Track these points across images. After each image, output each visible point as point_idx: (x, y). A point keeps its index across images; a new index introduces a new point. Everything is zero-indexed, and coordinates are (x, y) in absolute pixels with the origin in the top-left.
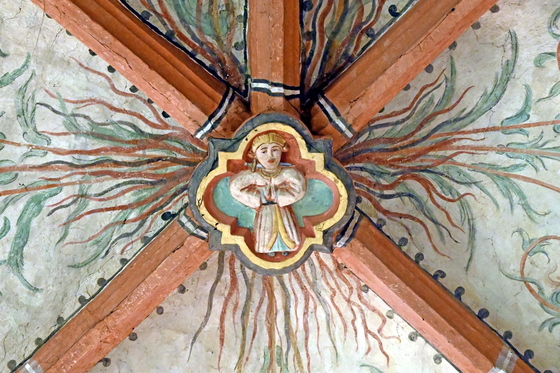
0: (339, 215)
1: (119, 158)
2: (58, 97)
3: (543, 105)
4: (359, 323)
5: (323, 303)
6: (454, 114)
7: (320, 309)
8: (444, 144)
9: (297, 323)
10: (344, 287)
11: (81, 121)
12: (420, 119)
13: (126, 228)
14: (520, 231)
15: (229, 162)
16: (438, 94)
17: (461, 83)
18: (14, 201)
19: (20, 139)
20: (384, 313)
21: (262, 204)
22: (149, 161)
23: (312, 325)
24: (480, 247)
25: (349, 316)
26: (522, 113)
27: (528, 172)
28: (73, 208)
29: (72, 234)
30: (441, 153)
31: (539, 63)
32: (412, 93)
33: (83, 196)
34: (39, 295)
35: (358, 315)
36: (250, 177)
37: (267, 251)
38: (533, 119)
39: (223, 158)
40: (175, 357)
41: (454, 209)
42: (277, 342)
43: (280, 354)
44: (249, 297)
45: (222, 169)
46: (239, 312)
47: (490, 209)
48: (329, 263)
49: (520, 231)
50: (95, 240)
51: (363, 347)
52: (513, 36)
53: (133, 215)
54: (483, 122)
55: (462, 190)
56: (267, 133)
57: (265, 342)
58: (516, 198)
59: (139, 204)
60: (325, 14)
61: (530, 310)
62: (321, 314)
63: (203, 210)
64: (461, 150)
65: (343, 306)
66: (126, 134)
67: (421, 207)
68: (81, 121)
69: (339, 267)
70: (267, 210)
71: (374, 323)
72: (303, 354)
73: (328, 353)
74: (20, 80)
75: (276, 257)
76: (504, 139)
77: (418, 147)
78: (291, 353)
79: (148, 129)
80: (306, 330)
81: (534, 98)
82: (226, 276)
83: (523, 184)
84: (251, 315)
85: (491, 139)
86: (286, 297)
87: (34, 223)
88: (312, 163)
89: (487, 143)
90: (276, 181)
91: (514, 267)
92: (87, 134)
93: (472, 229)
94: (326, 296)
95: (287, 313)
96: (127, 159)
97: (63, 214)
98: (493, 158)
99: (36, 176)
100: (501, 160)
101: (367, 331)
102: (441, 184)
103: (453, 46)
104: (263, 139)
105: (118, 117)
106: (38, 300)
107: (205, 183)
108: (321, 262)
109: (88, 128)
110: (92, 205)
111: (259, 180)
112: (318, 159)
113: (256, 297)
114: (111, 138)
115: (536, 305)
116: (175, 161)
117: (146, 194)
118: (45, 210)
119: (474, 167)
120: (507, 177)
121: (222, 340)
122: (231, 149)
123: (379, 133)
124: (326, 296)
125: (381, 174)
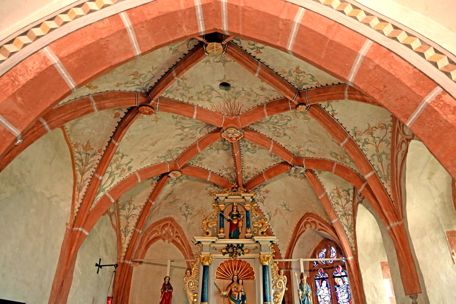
10: (219, 110)
23: (224, 105)
25: (218, 107)
44: (234, 107)
54: (202, 127)
62: (222, 106)
65: (219, 108)
70: (233, 133)
71: (214, 108)
76: (199, 126)
80: (224, 104)
85: (201, 126)
86: (228, 107)
88: (227, 139)
94: (222, 109)
113: (233, 107)
124: (222, 109)
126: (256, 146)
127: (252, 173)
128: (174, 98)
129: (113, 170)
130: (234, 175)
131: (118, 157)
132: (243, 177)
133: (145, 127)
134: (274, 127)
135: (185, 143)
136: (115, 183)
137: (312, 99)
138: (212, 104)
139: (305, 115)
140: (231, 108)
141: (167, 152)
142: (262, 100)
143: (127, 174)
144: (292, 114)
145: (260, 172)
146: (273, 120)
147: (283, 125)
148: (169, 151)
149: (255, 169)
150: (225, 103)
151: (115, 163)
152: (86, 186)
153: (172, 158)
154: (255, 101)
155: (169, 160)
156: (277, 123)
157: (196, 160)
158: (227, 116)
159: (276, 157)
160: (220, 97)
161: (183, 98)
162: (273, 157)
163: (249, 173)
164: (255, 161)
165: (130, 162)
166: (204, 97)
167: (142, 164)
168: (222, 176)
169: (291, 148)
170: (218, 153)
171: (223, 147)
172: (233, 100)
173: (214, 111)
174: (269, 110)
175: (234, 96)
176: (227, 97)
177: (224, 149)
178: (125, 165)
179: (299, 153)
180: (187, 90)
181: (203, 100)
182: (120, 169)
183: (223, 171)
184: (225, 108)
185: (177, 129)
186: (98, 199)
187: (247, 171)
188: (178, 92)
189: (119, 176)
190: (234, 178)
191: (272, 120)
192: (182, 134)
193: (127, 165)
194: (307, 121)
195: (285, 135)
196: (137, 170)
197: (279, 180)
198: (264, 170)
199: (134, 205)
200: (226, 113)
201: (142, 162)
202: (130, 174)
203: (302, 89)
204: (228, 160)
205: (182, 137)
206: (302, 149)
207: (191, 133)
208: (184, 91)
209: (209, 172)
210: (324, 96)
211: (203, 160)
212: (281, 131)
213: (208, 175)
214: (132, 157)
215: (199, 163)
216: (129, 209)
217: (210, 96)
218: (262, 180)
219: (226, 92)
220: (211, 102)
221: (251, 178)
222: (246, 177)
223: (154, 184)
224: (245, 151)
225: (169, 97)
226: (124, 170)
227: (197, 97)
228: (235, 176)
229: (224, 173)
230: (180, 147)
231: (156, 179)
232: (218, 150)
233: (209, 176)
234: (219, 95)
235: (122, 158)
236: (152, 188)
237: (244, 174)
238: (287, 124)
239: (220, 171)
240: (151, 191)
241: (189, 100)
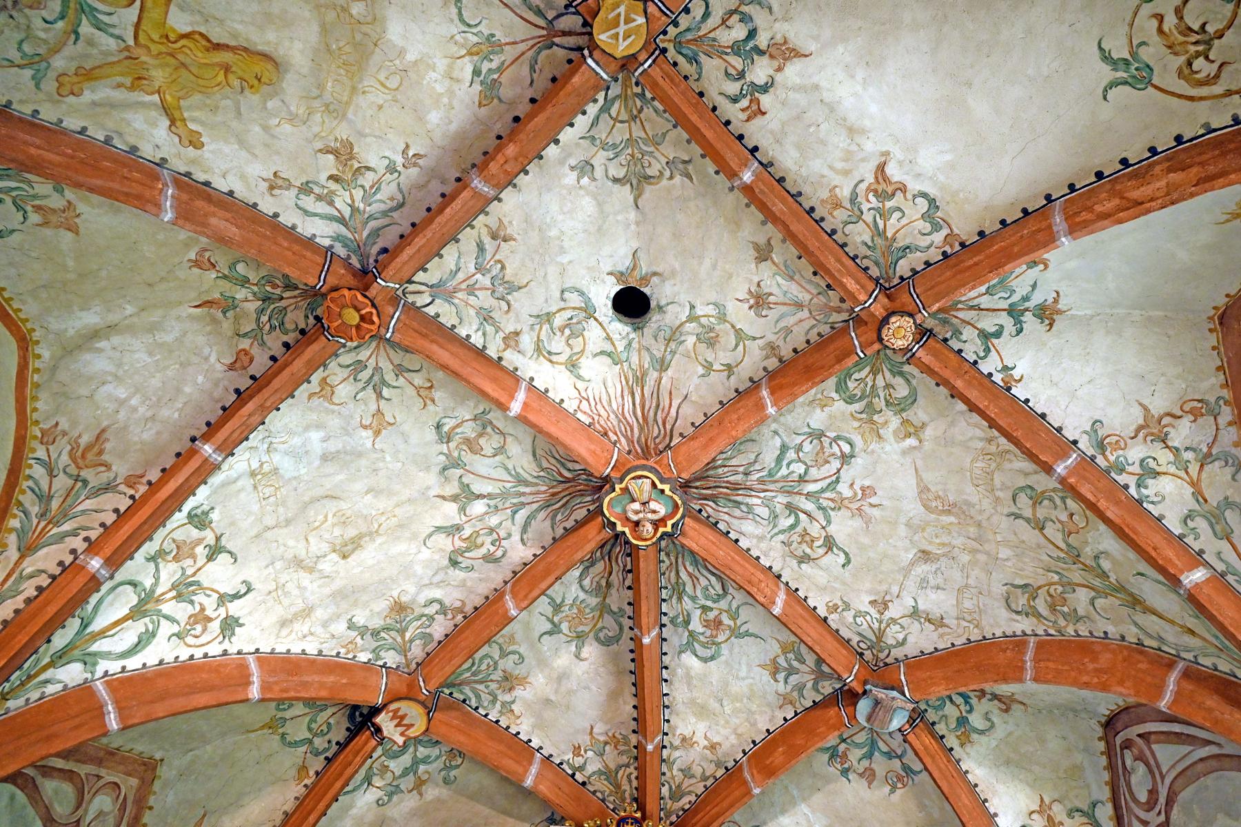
0: (607, 500)
1: (725, 490)
2: (756, 522)
3: (505, 518)
4: (593, 404)
5: (614, 412)
6: (550, 509)
7: (615, 409)
8: (553, 495)
9: (628, 399)
10: (602, 423)
11: (745, 510)
12: (568, 506)
13: (724, 456)
14: (508, 458)
15: (666, 526)
16: (559, 517)
17: (548, 523)
18: (783, 477)
19: (778, 505)
20: (579, 413)
21: (648, 502)
22: (710, 488)
23: (620, 400)
24: (529, 448)
25: (599, 407)
26: (515, 513)
27: (510, 485)
28: (752, 469)
29: (753, 457)
30: (555, 490)
31: (509, 535)
32: (573, 518)
33: (746, 474)
34: (773, 429)
35: (593, 408)
36: (655, 517)
37: (645, 480)
38: (509, 511)
39: (669, 529)
40: (697, 387)
41: (545, 464)
42: (639, 389)
43: (637, 382)
44: (656, 414)
45: (670, 523)
46: (661, 407)
47: (526, 466)
48: (611, 434)
49: (508, 458)
50: (740, 452)
51: (589, 391)
52: (524, 544)
53: (720, 462)
54: (535, 506)
55: (542, 474)
56: (646, 540)
57: (646, 388)
58: (513, 472)
59: (716, 468)
60: (620, 552)
61: (498, 419)
62: (615, 406)
63: (679, 502)
64: (544, 492)
66: (722, 502)
67: (563, 465)
68: (745, 510)
69: (606, 434)
72: (624, 383)
73: (609, 384)
74: (776, 530)
75: (640, 477)
76: (522, 499)
77: (567, 493)
78: (630, 383)
79: (711, 503)
80: (622, 396)
81: (510, 520)
82: (668, 427)
83: (510, 479)
84: (654, 405)
85: (530, 499)
87: (773, 465)
88: (623, 526)
89: (532, 497)
90: (641, 515)
91: (509, 439)
92: (742, 503)
93: (534, 455)
95: (634, 404)
96: (721, 490)
97: (757, 467)
98: (527, 490)
99: (771, 487)
100: (522, 489)
101: (588, 400)
102: (553, 476)
103: (554, 539)
104: (648, 537)
105: (725, 510)
106: (774, 426)
107: (678, 516)
108: (616, 434)
109: (742, 506)
110: (741, 469)
111: (650, 516)
112: (619, 528)
113: (652, 414)
114: (730, 500)
115: (495, 422)
116: (697, 488)
117: (711, 473)
118: (767, 470)
119: (537, 484)
120: (519, 481)
121: (671, 393)
122: (664, 534)
123: (589, 498)
124: (612, 416)
125: (586, 480)
126: (720, 623)
127: (697, 771)
128: (454, 326)
129: (159, 591)
130: (630, 781)
131: (200, 541)
132: (665, 791)
133: (333, 446)
134: (791, 508)
135: (463, 584)
136: (150, 657)
137: (936, 289)
138: (581, 385)
139: (904, 415)
140: (645, 418)
141: (392, 609)
142: (753, 361)
143: (209, 645)
144: (856, 424)
145: (730, 764)
146: (788, 465)
147: (823, 491)
148: (400, 608)
149: (713, 747)
150: (626, 393)
151: (176, 559)
152: (21, 598)
153: (404, 651)
154: (729, 368)
155: (391, 658)
156: (802, 479)
157: (493, 686)
158: (629, 452)
159: (794, 679)
160: (609, 355)
161: (484, 334)
162: (781, 676)
163: (687, 772)
164: (714, 705)
165: (237, 596)
166: (558, 344)
167: (284, 632)
168: (584, 784)
169: (849, 616)
170: (578, 656)
171: (600, 625)
172: (655, 375)
173: (587, 421)
174: (781, 387)
175: (658, 355)
176: (635, 359)
177: (601, 635)
178: (216, 596)
179: (880, 635)
180: (503, 299)
181: (554, 358)
182: (192, 602)
183: (590, 754)
184: (621, 417)
185: (443, 498)
187: (680, 757)
188: (472, 300)
189: (178, 635)
190: (627, 795)
191: (784, 471)
192: (458, 528)
193: (223, 599)
194: (911, 442)
195: (830, 544)
196: (257, 651)
197: (804, 808)
198: (745, 753)
200: (623, 440)
201: (284, 623)
202: (225, 653)
203: (896, 281)
204: (614, 696)
205: (458, 543)
206: (894, 611)
207: (492, 530)
208: (495, 303)
209: (533, 754)
210: (976, 264)
211: (518, 692)
212: (815, 530)
213: (530, 764)
214: (251, 572)
215: (504, 704)
217: (577, 343)
218: (737, 793)
219: (633, 335)
220: (579, 377)
221: (693, 798)
222: (676, 795)
223: (312, 773)
224: (680, 652)
225: (438, 315)
226: (201, 618)
227: (535, 335)
228: (635, 784)
229: (591, 768)
230: (440, 602)
231: (326, 750)
232: (580, 637)
233: (534, 770)
234: (609, 348)
235: (210, 558)
236: (299, 790)
237: (668, 774)
238: (837, 481)
239: (579, 755)
240: (289, 806)
241: (507, 346)
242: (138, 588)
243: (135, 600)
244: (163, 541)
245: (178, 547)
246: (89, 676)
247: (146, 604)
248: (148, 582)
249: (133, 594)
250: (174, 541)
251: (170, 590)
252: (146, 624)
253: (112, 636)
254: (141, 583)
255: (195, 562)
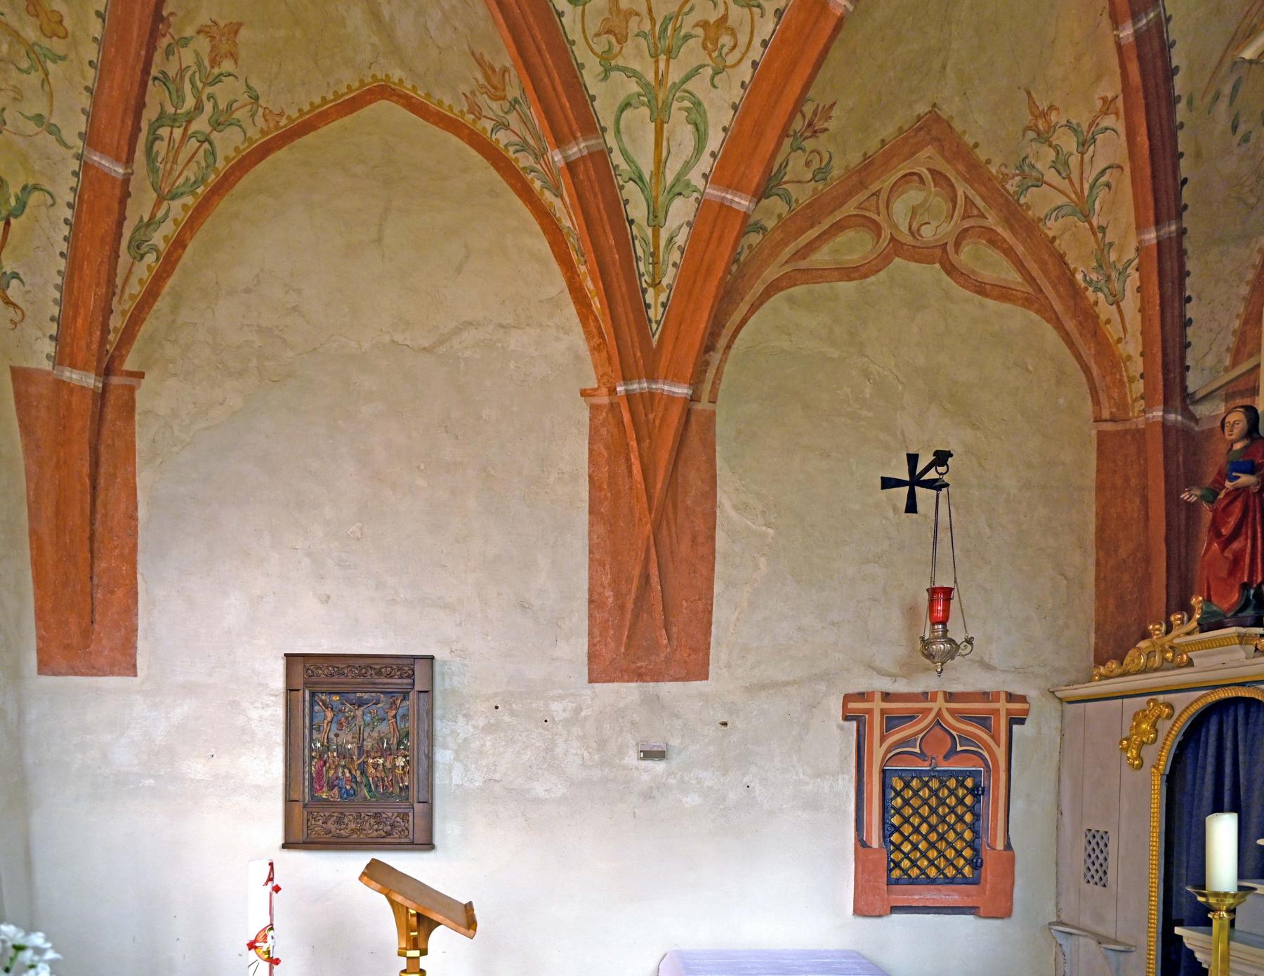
129: (650, 77)
136: (719, 119)
151: (622, 40)
186: (681, 239)
199: (1069, 125)
216: (1061, 164)
242: (633, 102)
243: (646, 111)
244: (592, 50)
245: (609, 32)
246: (696, 195)
247: (656, 99)
248: (634, 87)
249: (636, 111)
250: (598, 35)
251: (657, 62)
252: (680, 109)
253: (669, 153)
254: (629, 96)
255: (637, 14)
